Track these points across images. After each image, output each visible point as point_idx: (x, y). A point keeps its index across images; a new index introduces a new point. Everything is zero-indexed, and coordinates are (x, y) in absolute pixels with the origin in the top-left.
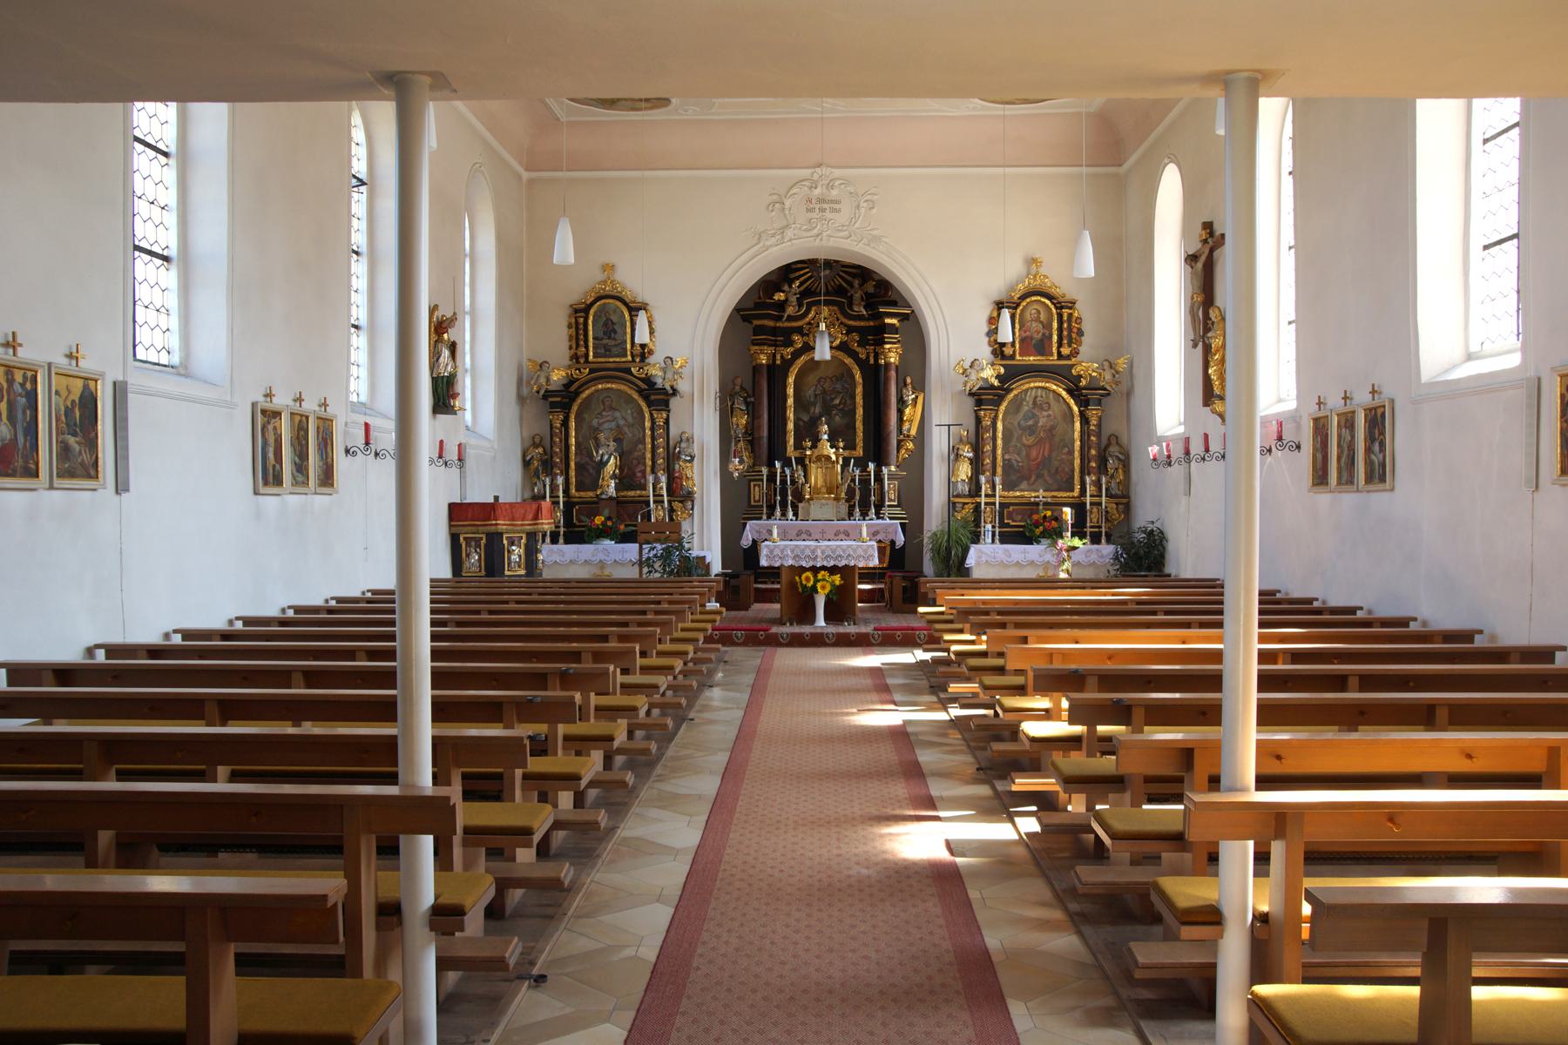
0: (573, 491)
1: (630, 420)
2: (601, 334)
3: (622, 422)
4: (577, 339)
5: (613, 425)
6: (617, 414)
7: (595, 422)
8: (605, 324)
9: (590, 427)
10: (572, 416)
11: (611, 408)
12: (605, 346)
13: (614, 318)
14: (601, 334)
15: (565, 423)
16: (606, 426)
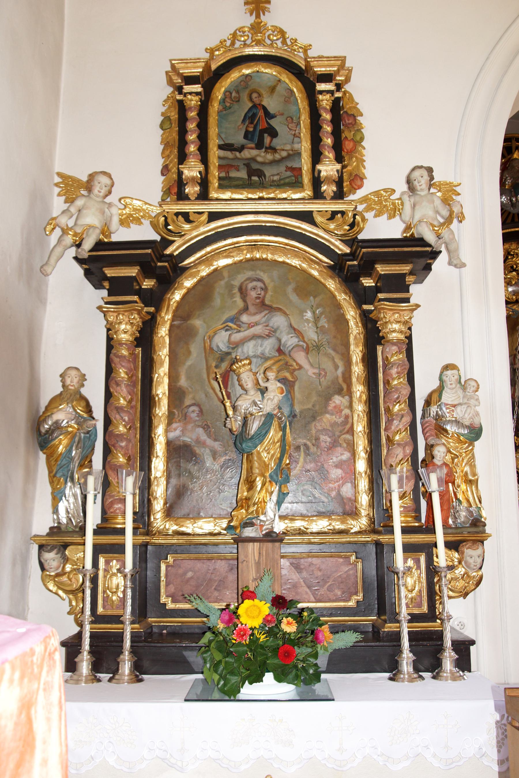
0: (158, 520)
1: (311, 334)
2: (239, 139)
3: (290, 341)
4: (183, 143)
5: (268, 346)
6: (278, 321)
7: (221, 340)
8: (250, 117)
9: (209, 351)
10: (167, 317)
11: (263, 306)
12: (248, 164)
13: (271, 104)
14: (239, 139)
15: (145, 339)
16: (249, 348)
